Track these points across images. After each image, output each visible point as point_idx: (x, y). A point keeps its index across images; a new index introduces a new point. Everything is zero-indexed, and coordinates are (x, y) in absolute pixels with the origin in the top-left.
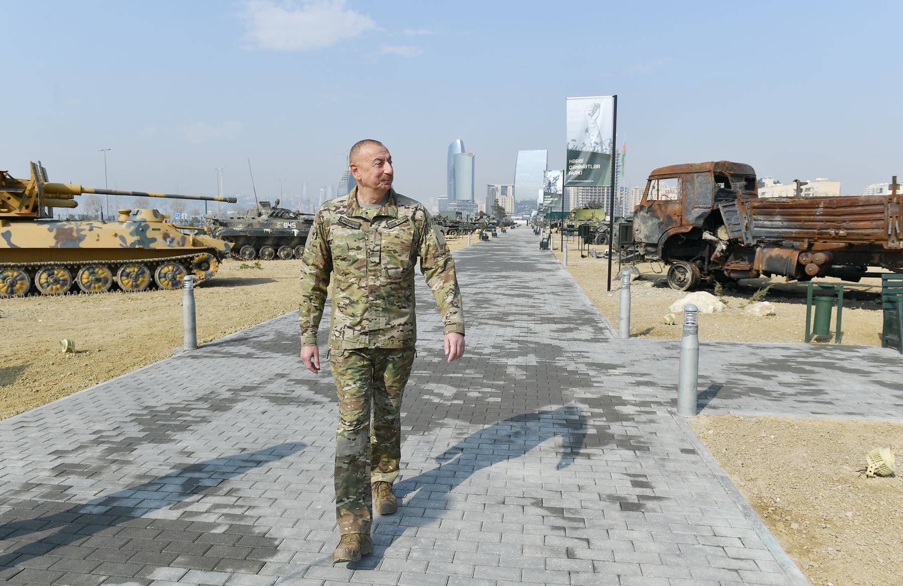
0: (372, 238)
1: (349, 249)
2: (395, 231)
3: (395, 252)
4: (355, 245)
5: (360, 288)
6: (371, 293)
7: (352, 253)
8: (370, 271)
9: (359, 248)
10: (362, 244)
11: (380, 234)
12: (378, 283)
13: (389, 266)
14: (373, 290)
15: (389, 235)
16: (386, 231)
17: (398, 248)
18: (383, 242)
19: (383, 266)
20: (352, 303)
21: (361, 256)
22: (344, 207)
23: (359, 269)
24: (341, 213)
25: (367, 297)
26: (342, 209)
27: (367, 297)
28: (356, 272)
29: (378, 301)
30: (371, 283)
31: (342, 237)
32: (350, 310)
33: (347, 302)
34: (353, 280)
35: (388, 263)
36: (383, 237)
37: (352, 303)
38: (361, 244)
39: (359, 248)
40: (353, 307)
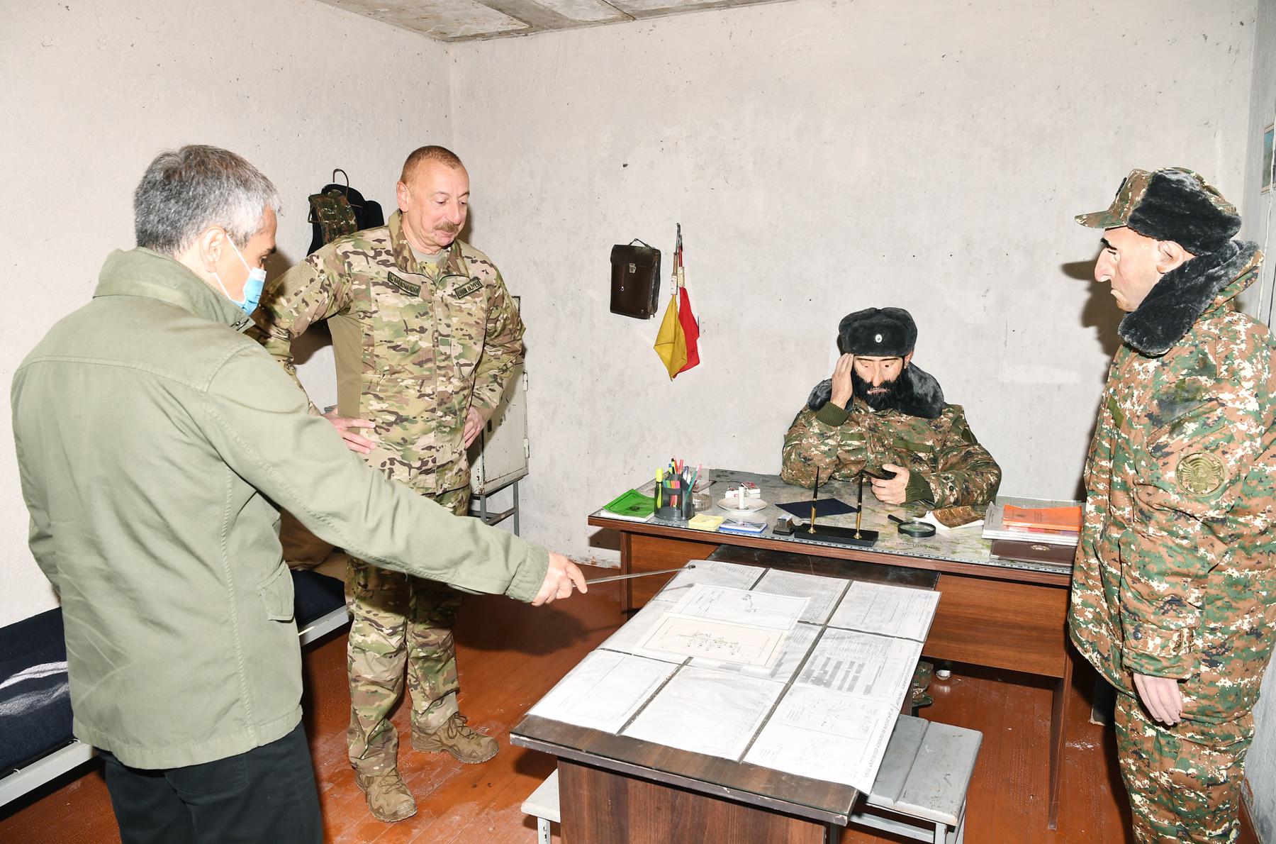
0: (439, 312)
3: (471, 338)
4: (415, 323)
6: (440, 405)
7: (413, 338)
8: (439, 368)
9: (422, 330)
10: (427, 324)
12: (450, 389)
13: (462, 361)
14: (443, 400)
15: (461, 310)
16: (454, 302)
17: (473, 332)
18: (455, 320)
19: (455, 361)
20: (401, 420)
21: (426, 344)
22: (388, 253)
23: (421, 364)
24: (385, 263)
25: (433, 411)
26: (384, 257)
27: (433, 411)
28: (417, 370)
29: (448, 418)
30: (441, 388)
31: (396, 308)
32: (397, 433)
33: (392, 418)
34: (409, 382)
35: (461, 356)
36: (453, 313)
37: (401, 420)
38: (427, 324)
39: (422, 330)
40: (405, 429)
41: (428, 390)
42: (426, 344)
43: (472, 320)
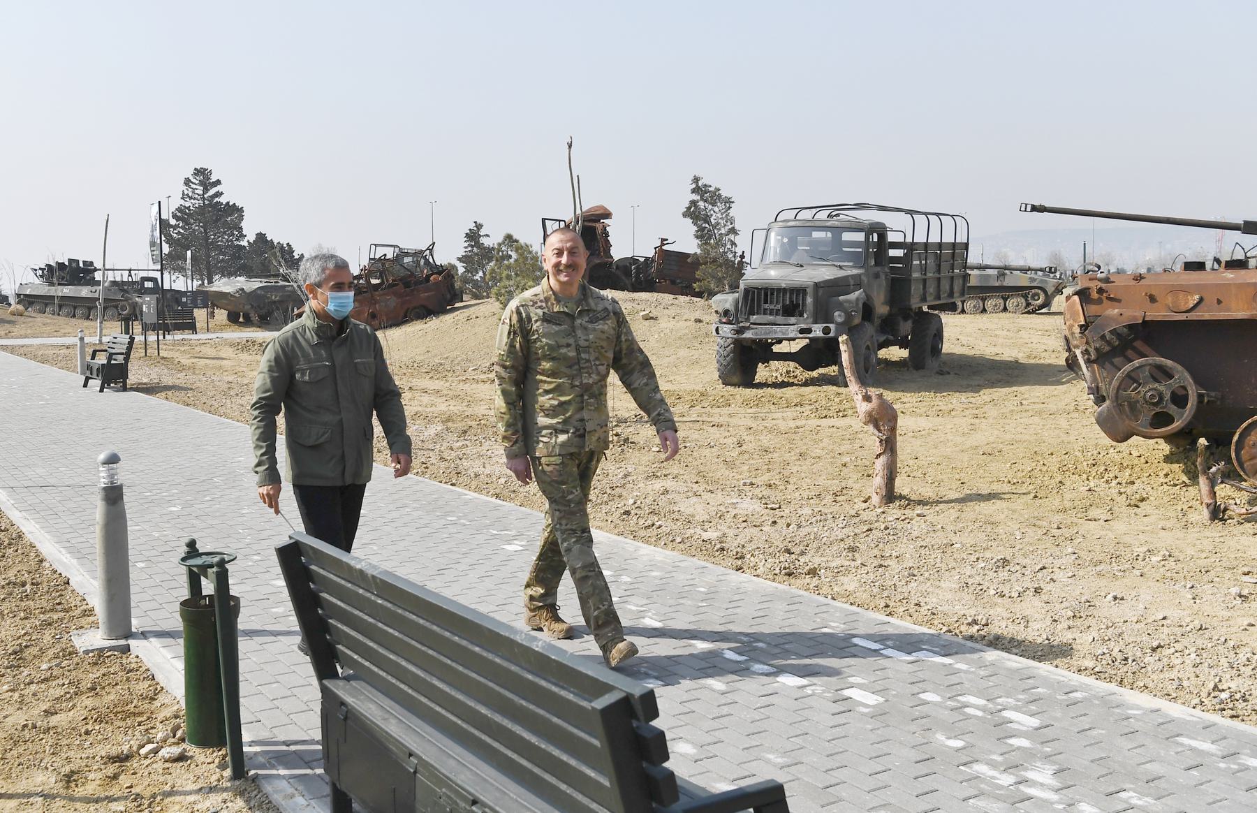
0: (579, 333)
1: (559, 347)
2: (600, 326)
4: (564, 341)
5: (573, 386)
7: (563, 351)
9: (568, 345)
10: (571, 341)
11: (586, 328)
12: (591, 381)
15: (595, 330)
17: (604, 344)
21: (572, 354)
23: (570, 367)
24: (540, 307)
25: (582, 396)
28: (567, 371)
35: (597, 359)
38: (571, 341)
39: (568, 345)
41: (577, 383)
42: (572, 354)
43: (604, 336)
